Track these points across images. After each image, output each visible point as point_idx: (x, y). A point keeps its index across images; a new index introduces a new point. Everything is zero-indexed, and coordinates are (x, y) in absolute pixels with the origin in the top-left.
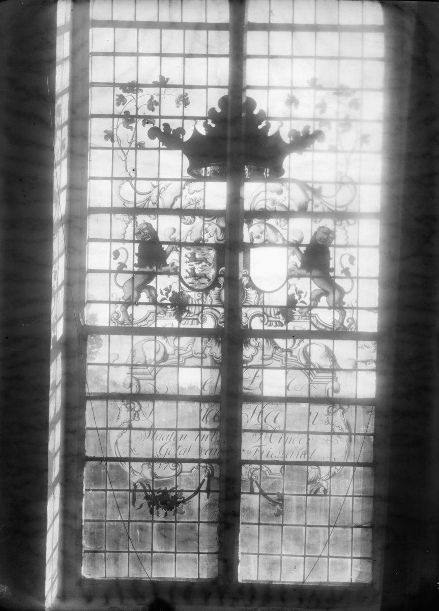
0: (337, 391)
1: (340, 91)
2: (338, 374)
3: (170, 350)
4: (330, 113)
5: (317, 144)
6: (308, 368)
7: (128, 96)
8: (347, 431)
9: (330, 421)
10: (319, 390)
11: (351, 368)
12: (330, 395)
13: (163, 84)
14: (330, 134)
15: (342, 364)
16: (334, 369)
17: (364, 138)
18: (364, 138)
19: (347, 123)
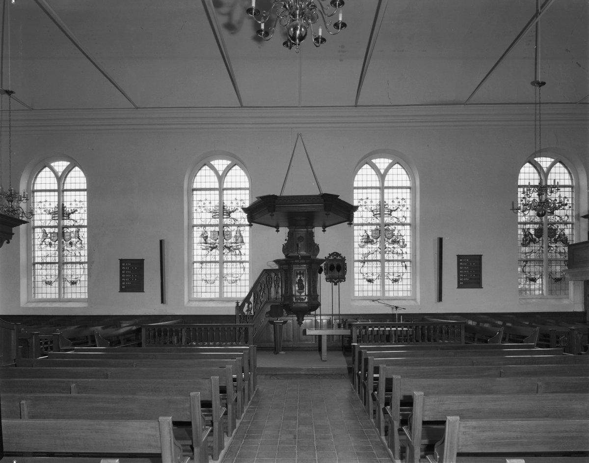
1: (403, 199)
3: (370, 251)
4: (400, 204)
5: (398, 210)
6: (397, 253)
7: (361, 201)
10: (400, 258)
13: (367, 199)
14: (401, 208)
15: (404, 253)
16: (402, 253)
17: (407, 208)
18: (407, 208)
19: (404, 206)
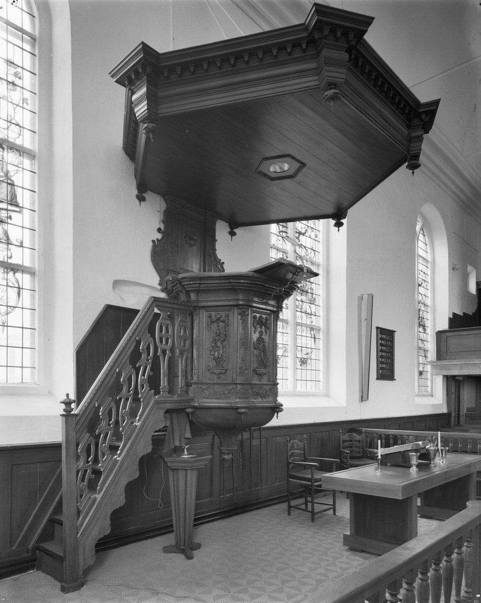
0: (11, 257)
2: (10, 246)
8: (17, 286)
9: (6, 277)
11: (19, 245)
12: (6, 261)
